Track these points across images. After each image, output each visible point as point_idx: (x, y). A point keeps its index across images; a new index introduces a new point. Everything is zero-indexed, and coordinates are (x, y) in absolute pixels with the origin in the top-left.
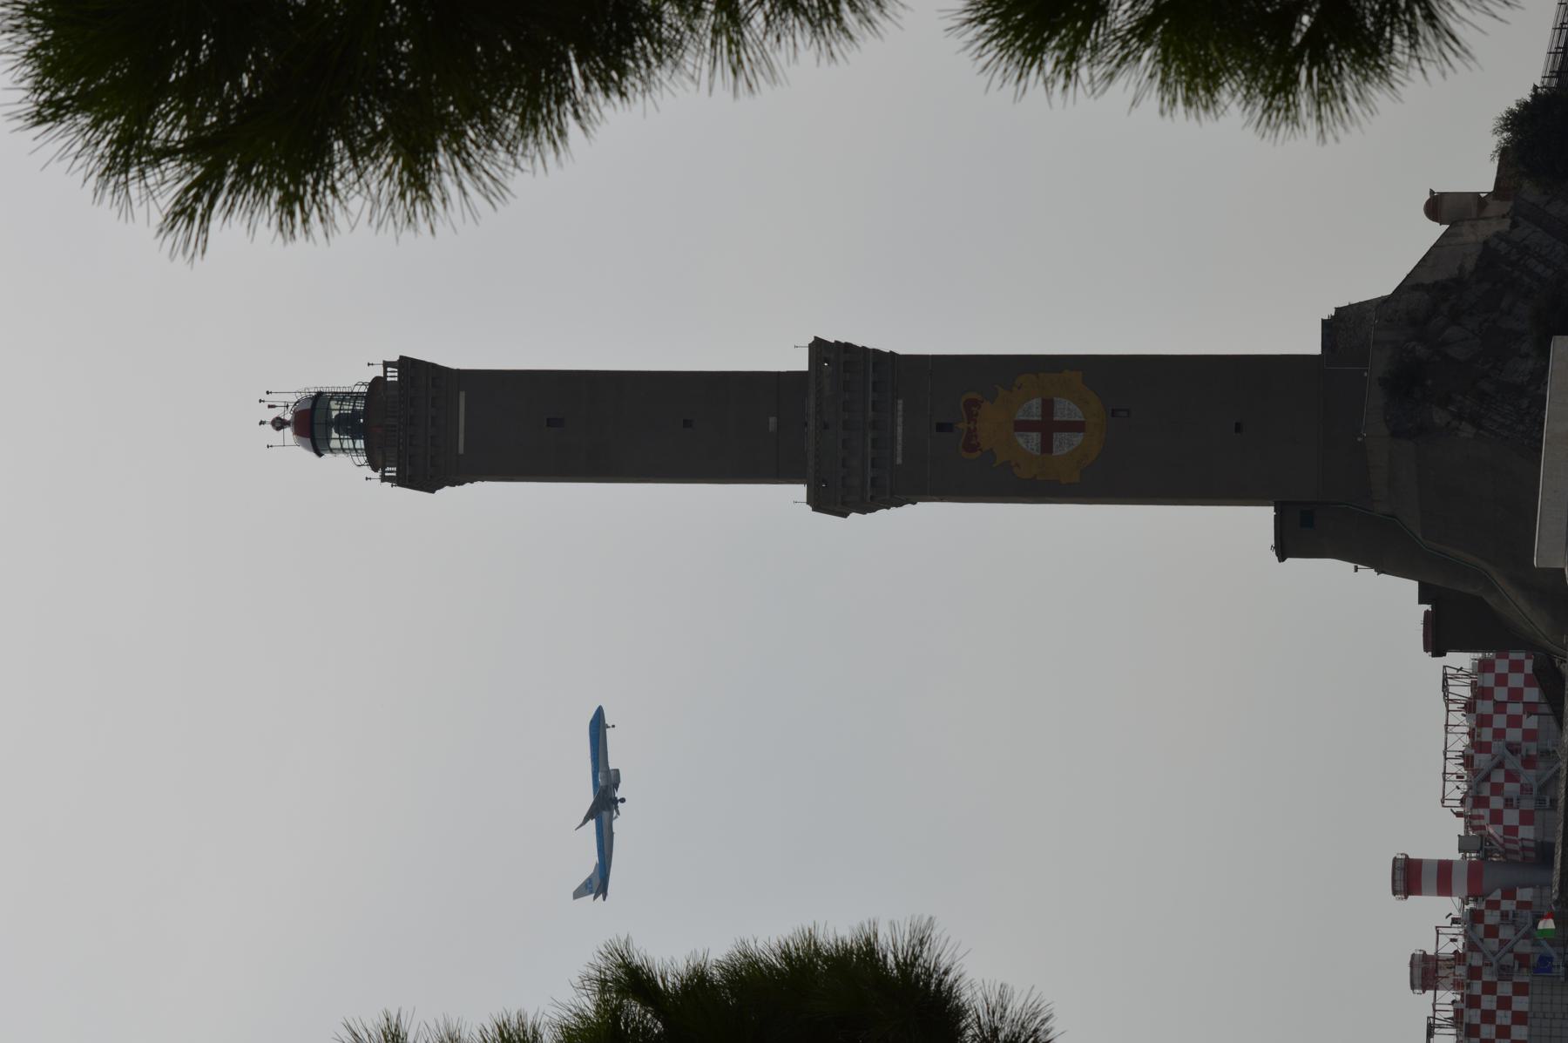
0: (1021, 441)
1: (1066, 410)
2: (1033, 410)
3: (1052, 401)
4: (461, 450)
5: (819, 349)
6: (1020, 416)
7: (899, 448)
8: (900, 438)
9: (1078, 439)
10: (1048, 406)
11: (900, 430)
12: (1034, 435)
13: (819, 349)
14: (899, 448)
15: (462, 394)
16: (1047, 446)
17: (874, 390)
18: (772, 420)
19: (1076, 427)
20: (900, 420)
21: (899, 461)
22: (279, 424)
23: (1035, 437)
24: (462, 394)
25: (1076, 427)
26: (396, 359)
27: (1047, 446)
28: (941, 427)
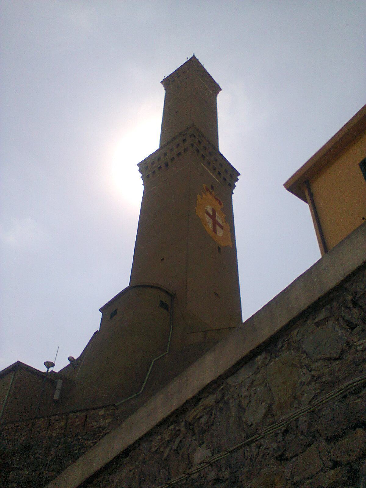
9: (211, 226)
23: (211, 213)
27: (207, 213)
28: (212, 187)
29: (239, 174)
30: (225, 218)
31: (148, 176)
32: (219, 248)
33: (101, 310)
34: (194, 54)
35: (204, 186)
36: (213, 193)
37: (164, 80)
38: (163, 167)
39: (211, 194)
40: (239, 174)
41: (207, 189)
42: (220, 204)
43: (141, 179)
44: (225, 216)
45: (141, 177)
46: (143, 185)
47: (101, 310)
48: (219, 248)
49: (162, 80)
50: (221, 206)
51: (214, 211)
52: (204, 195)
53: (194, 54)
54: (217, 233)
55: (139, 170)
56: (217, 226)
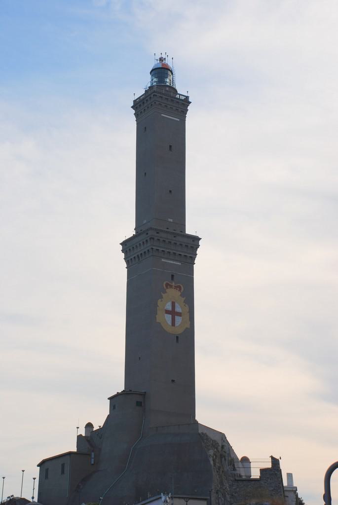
1: (178, 320)
2: (178, 309)
3: (181, 316)
4: (163, 115)
5: (197, 239)
6: (176, 304)
8: (169, 262)
9: (170, 323)
13: (197, 239)
15: (178, 120)
16: (167, 312)
18: (171, 220)
19: (173, 324)
21: (163, 260)
22: (161, 59)
24: (178, 120)
25: (173, 324)
27: (167, 312)
30: (184, 302)
31: (128, 261)
33: (109, 399)
35: (165, 283)
36: (173, 284)
37: (135, 101)
38: (137, 259)
39: (171, 286)
41: (167, 285)
42: (180, 290)
44: (184, 299)
47: (109, 399)
48: (177, 337)
49: (132, 104)
52: (164, 295)
55: (122, 250)
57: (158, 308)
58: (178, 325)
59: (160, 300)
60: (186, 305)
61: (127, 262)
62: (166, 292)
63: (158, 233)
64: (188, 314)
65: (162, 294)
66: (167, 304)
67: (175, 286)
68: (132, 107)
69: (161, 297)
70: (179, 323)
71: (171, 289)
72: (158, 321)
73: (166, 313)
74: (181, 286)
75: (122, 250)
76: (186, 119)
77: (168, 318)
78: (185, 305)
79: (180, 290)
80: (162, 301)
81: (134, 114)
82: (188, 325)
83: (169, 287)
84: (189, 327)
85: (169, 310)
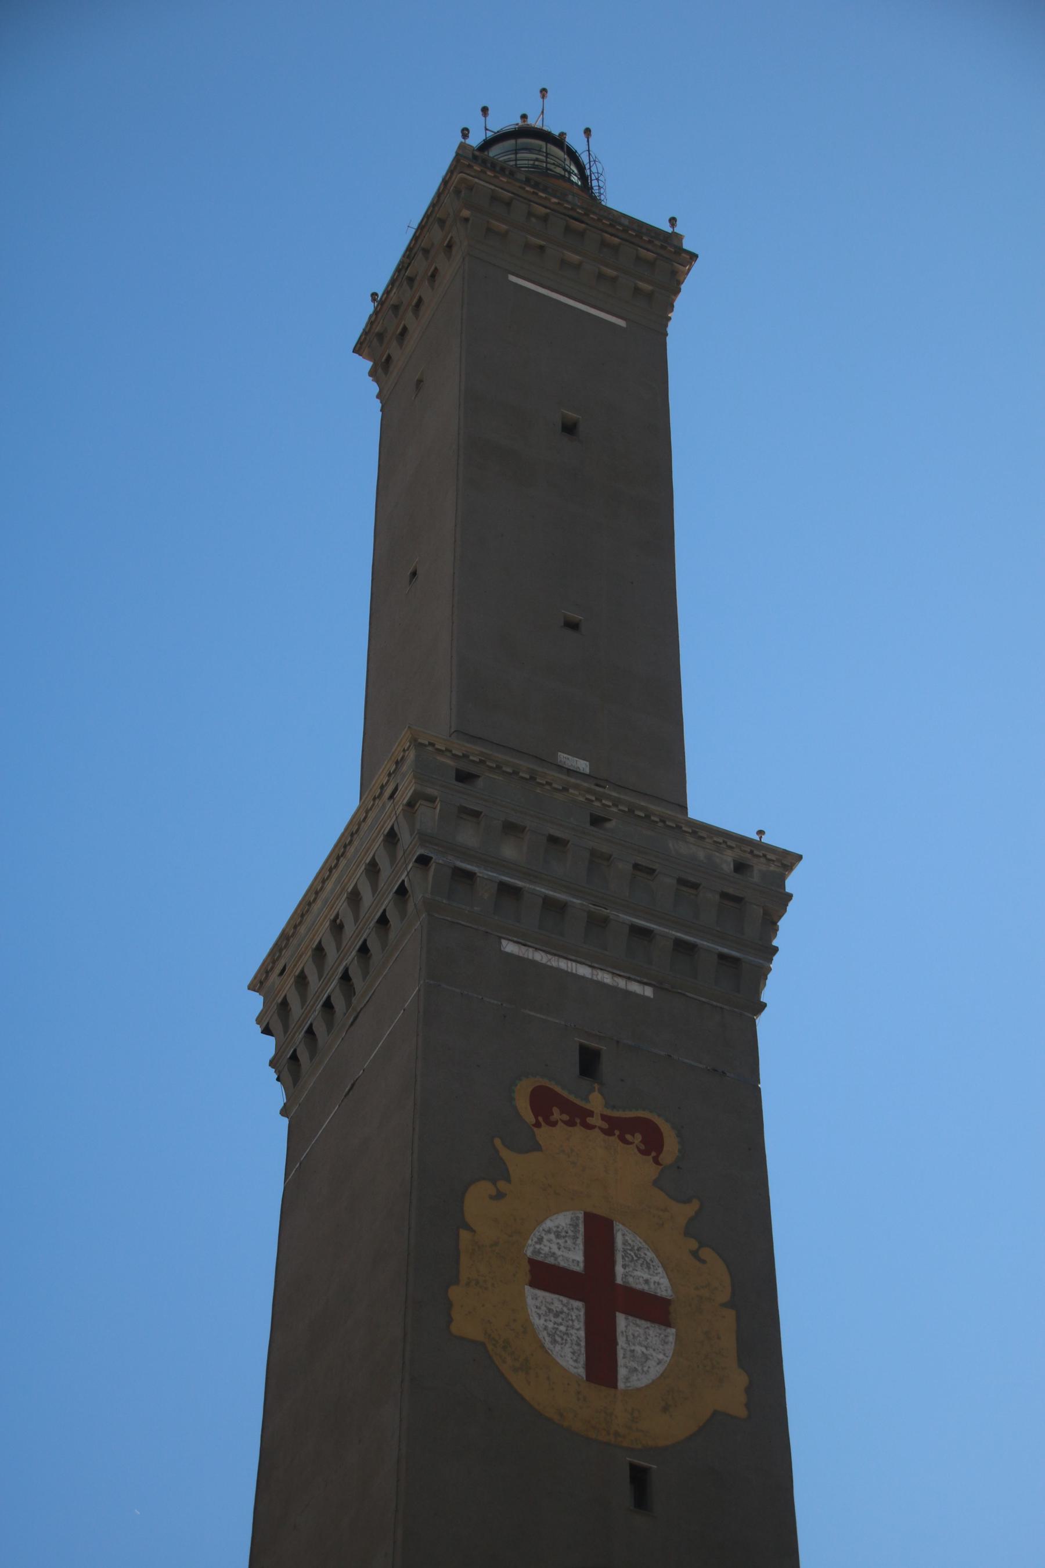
0: (562, 1220)
1: (644, 1352)
2: (639, 1270)
6: (621, 1236)
7: (539, 957)
8: (563, 964)
9: (570, 1357)
10: (653, 1309)
11: (584, 971)
12: (579, 1257)
14: (539, 957)
15: (622, 323)
16: (547, 1276)
17: (679, 943)
18: (583, 766)
20: (607, 978)
21: (509, 947)
23: (572, 1256)
24: (622, 323)
26: (687, 245)
27: (547, 1276)
28: (589, 1063)
29: (788, 861)
30: (687, 1233)
31: (294, 1057)
32: (639, 1477)
34: (465, 133)
36: (596, 1102)
39: (578, 1116)
40: (788, 861)
41: (544, 1102)
42: (652, 1143)
43: (272, 1074)
45: (273, 1063)
46: (284, 1112)
48: (639, 1477)
50: (656, 1161)
51: (598, 1233)
52: (515, 1162)
53: (465, 133)
54: (622, 1372)
56: (621, 1320)
57: (464, 1234)
58: (639, 1381)
59: (484, 1188)
60: (706, 1253)
61: (288, 1067)
62: (537, 1147)
63: (464, 777)
64: (731, 1315)
65: (505, 1154)
66: (548, 1224)
67: (604, 1117)
68: (358, 349)
69: (499, 1172)
70: (654, 1371)
71: (578, 1131)
72: (465, 1325)
73: (534, 1284)
74: (666, 1128)
75: (259, 1021)
76: (669, 330)
77: (557, 1326)
78: (695, 1254)
79: (652, 1144)
80: (500, 1196)
81: (372, 373)
82: (732, 1395)
83: (556, 1114)
84: (742, 1412)
85: (563, 1264)
